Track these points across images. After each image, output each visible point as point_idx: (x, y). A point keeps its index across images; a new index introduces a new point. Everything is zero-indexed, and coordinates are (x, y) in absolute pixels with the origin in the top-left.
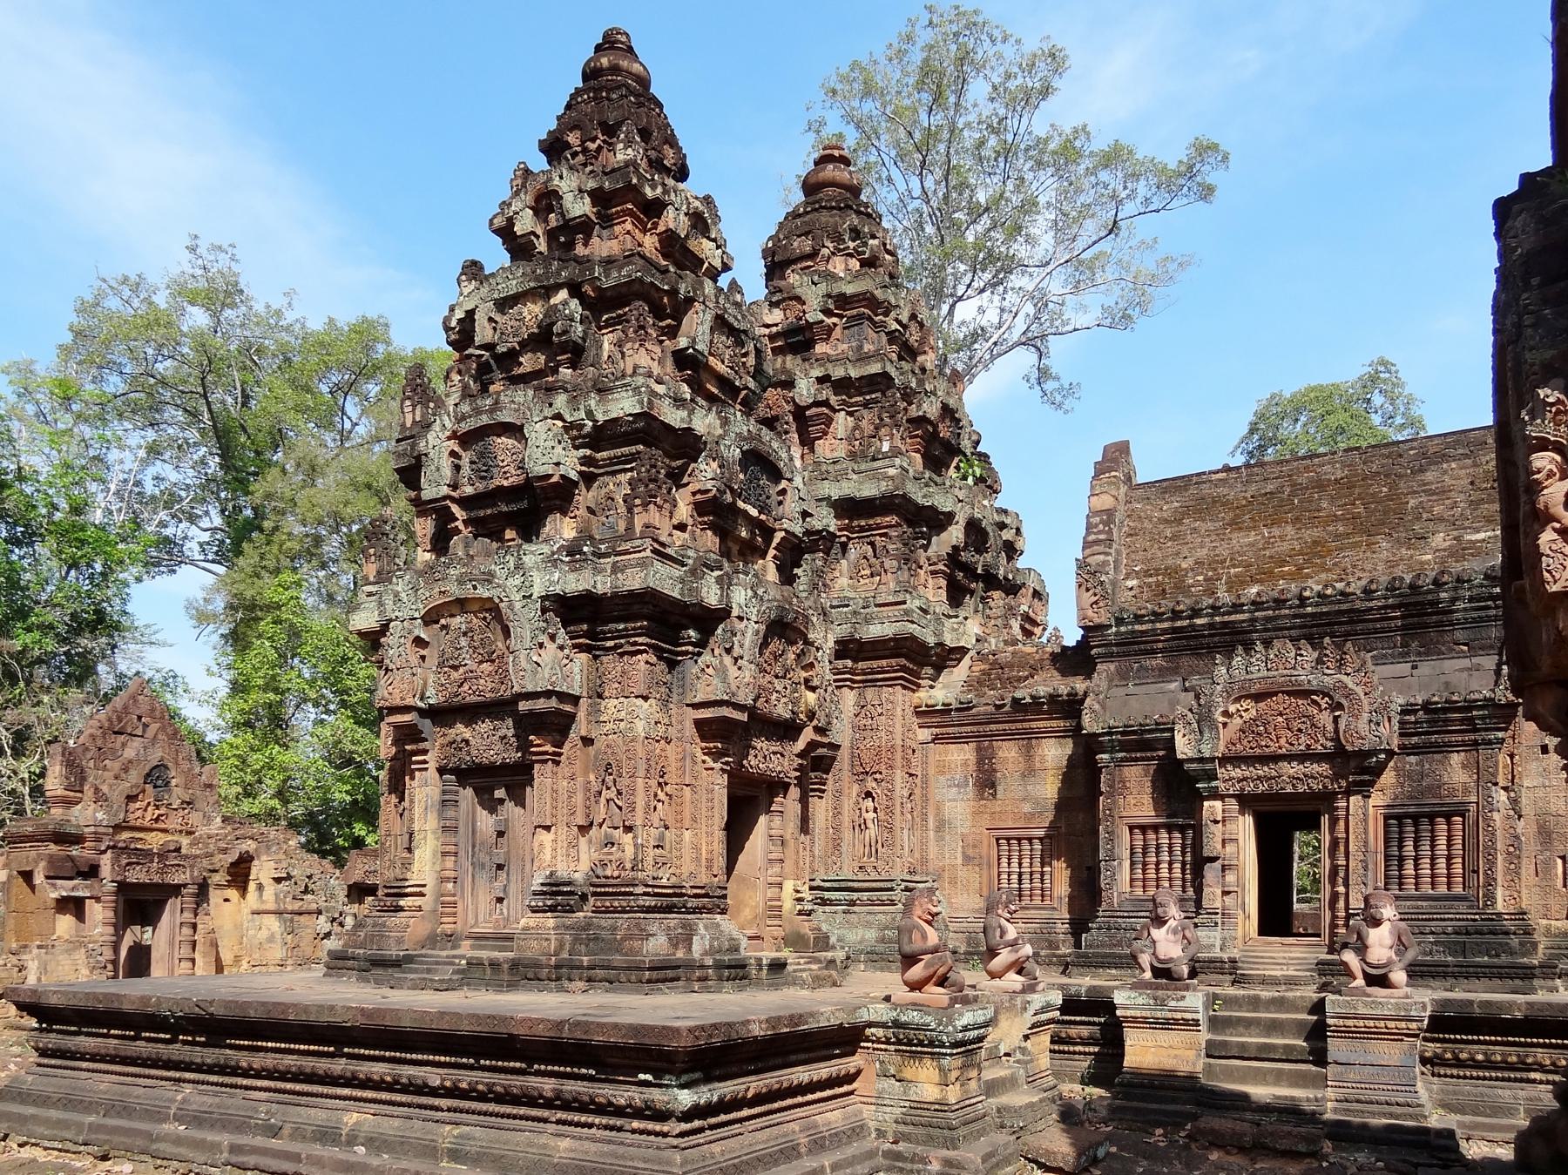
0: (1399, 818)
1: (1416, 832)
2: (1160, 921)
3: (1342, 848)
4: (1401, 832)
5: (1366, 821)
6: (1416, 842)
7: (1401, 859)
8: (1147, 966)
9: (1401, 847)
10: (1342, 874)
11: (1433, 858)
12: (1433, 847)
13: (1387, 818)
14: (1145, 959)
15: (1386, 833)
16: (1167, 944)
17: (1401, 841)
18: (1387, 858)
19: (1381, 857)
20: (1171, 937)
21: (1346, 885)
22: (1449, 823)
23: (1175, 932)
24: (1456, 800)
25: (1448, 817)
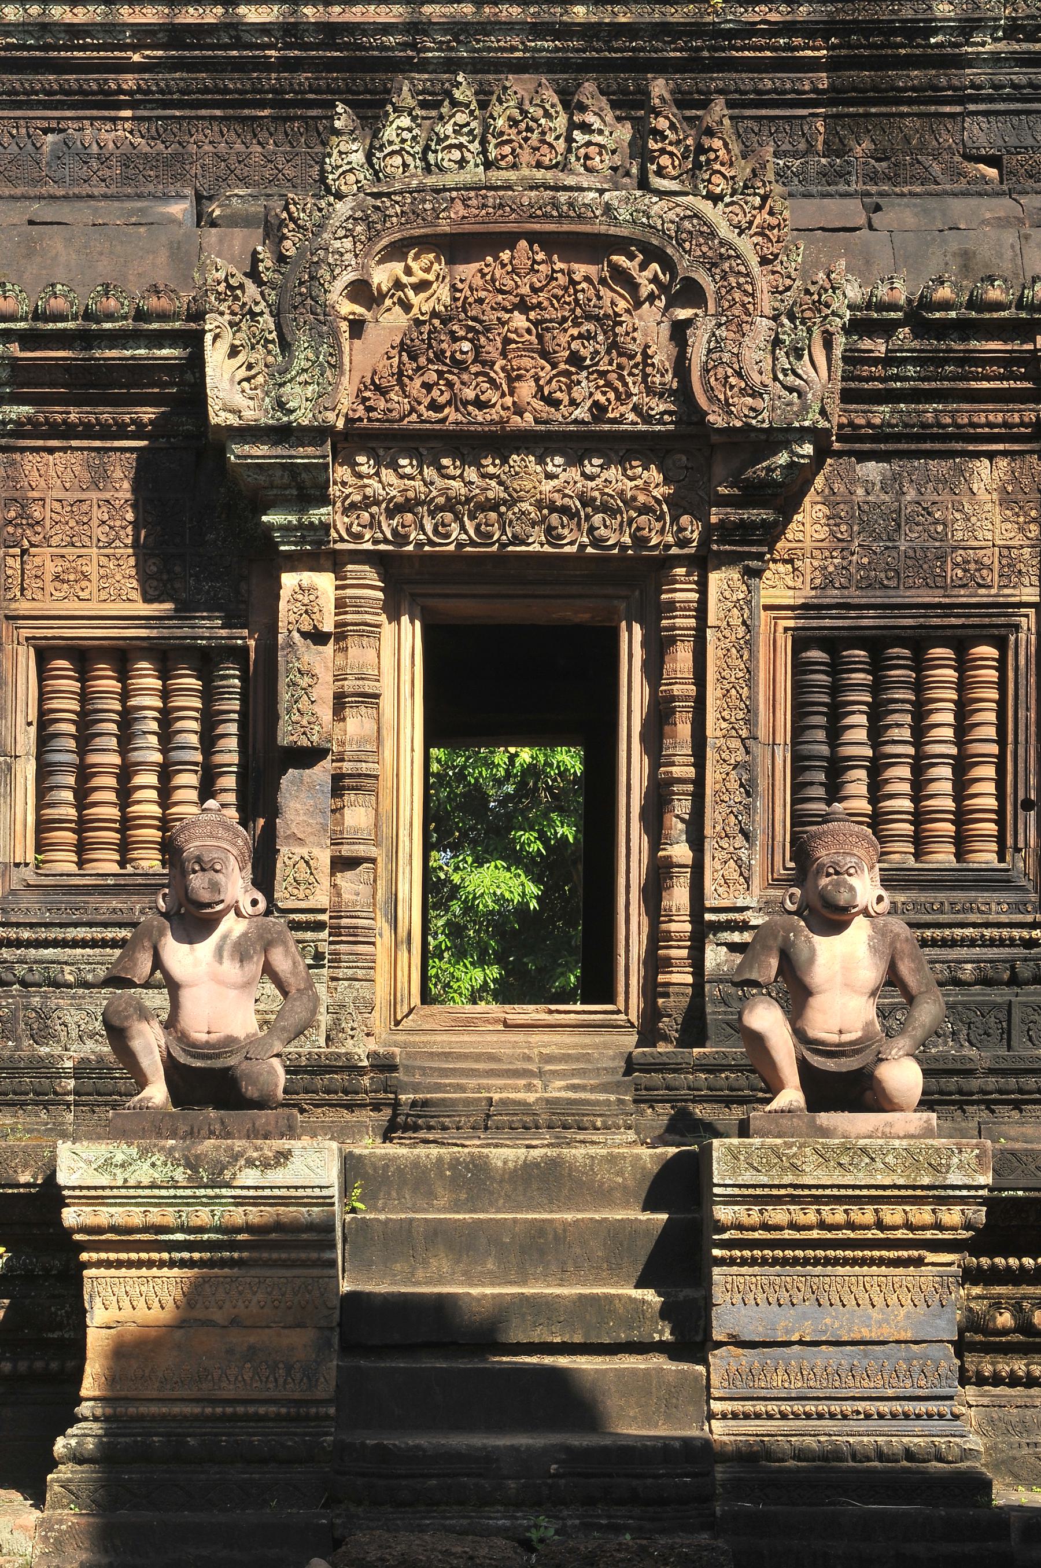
0: (833, 644)
1: (877, 688)
2: (194, 920)
3: (684, 729)
4: (836, 689)
5: (750, 644)
6: (877, 715)
7: (836, 769)
8: (152, 1063)
9: (835, 732)
10: (682, 806)
11: (920, 766)
12: (920, 732)
13: (801, 642)
14: (149, 1043)
15: (799, 688)
16: (215, 992)
17: (836, 714)
18: (800, 763)
19: (783, 756)
20: (230, 969)
21: (696, 841)
22: (963, 664)
23: (242, 952)
24: (983, 596)
25: (961, 645)
